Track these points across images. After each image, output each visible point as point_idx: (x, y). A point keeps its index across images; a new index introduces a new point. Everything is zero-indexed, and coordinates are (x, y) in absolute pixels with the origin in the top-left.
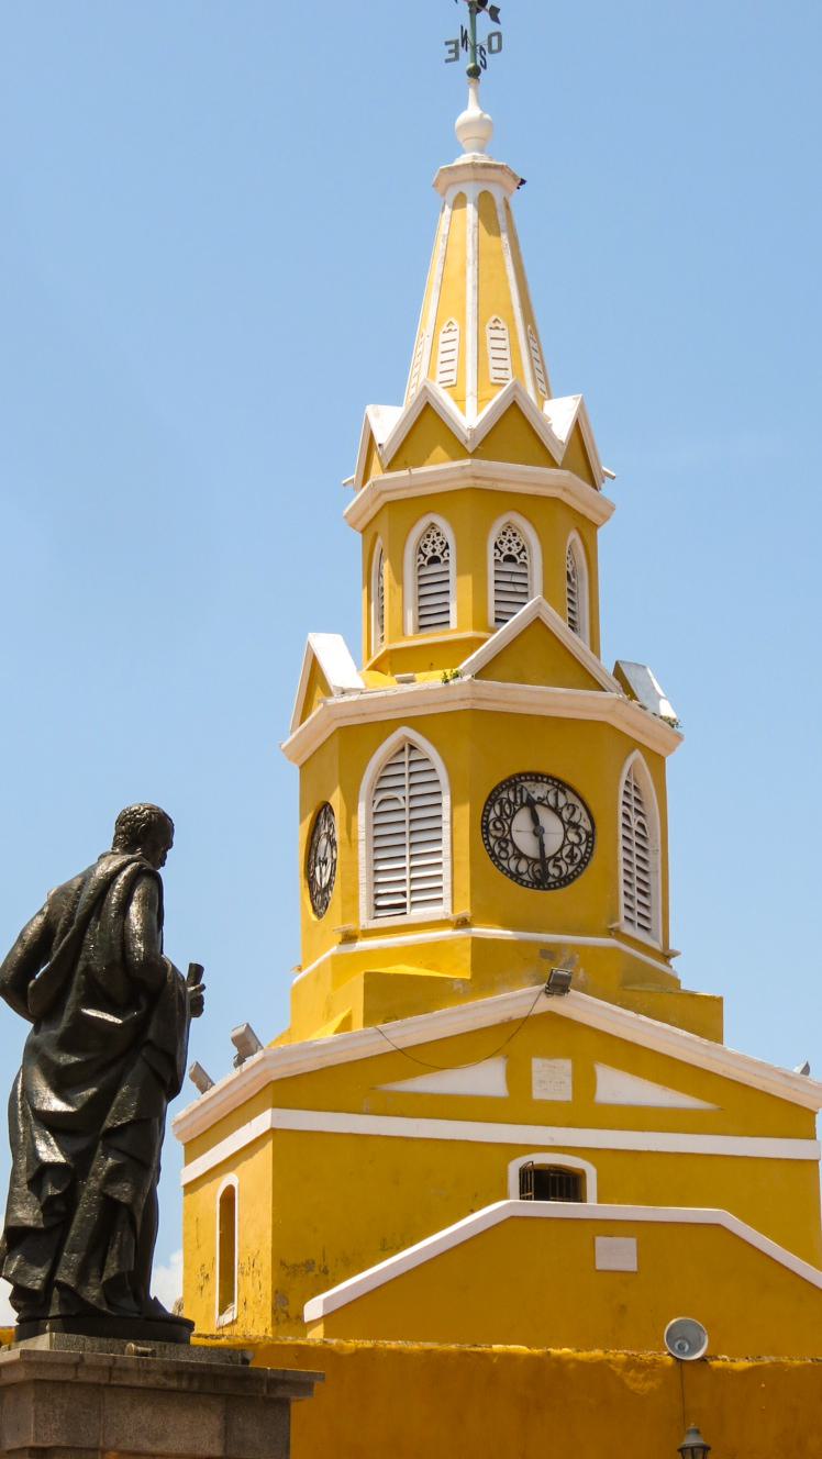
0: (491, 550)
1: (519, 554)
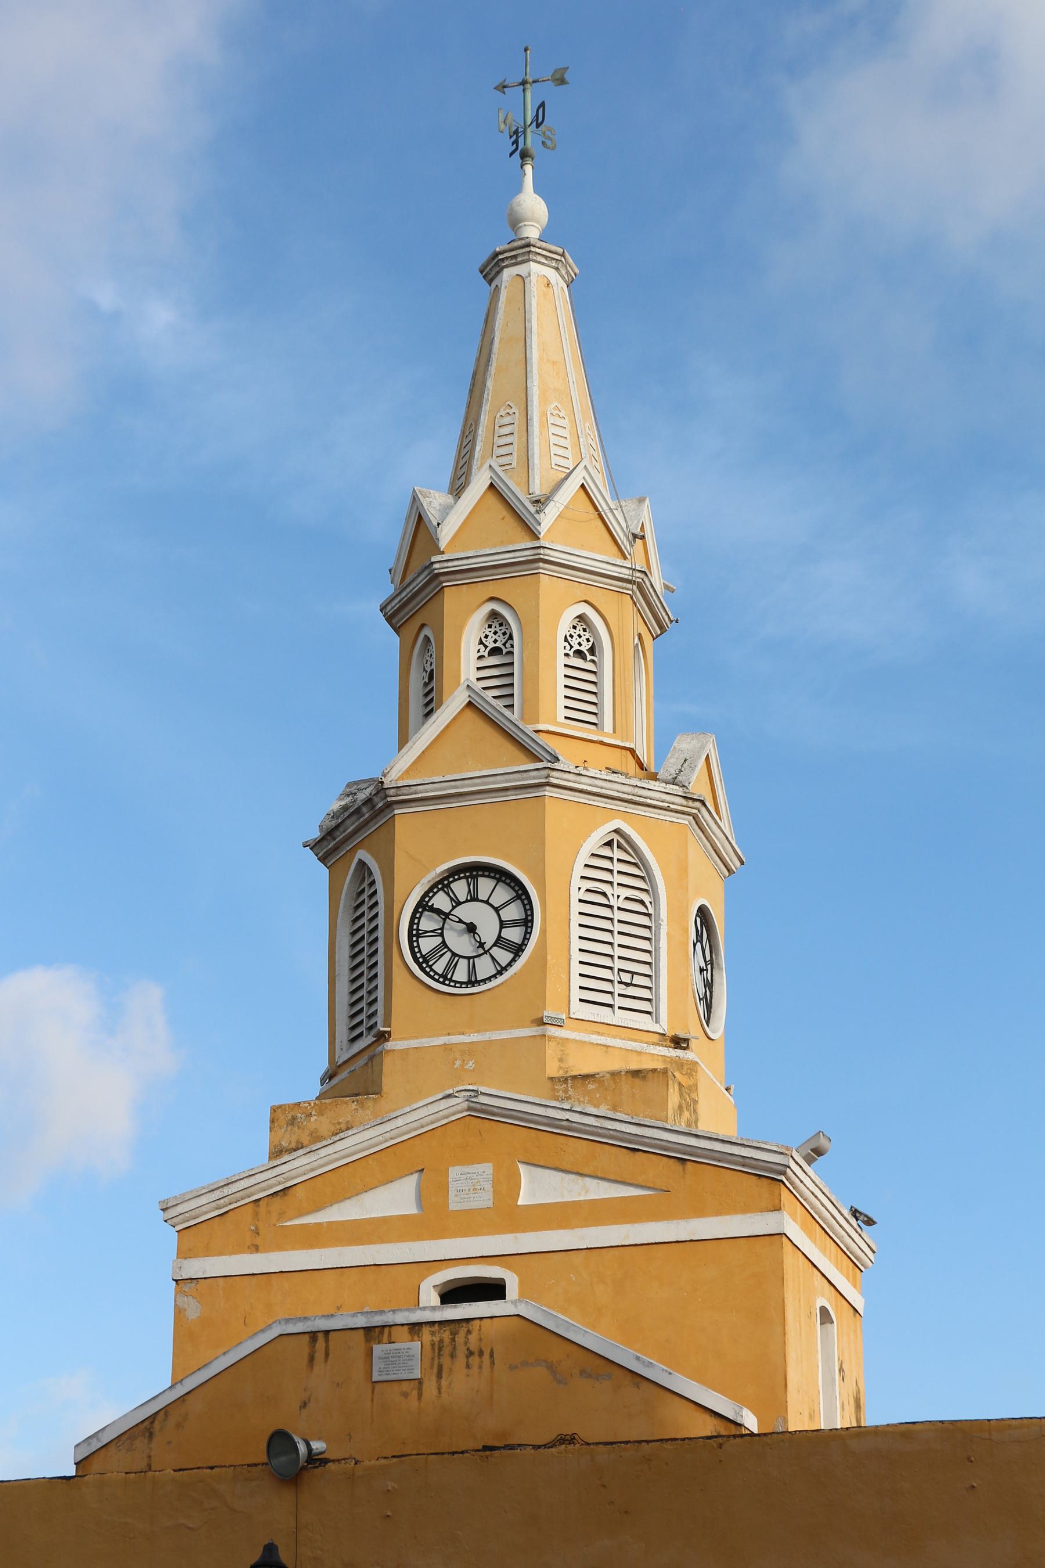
0: (561, 643)
1: (504, 644)
